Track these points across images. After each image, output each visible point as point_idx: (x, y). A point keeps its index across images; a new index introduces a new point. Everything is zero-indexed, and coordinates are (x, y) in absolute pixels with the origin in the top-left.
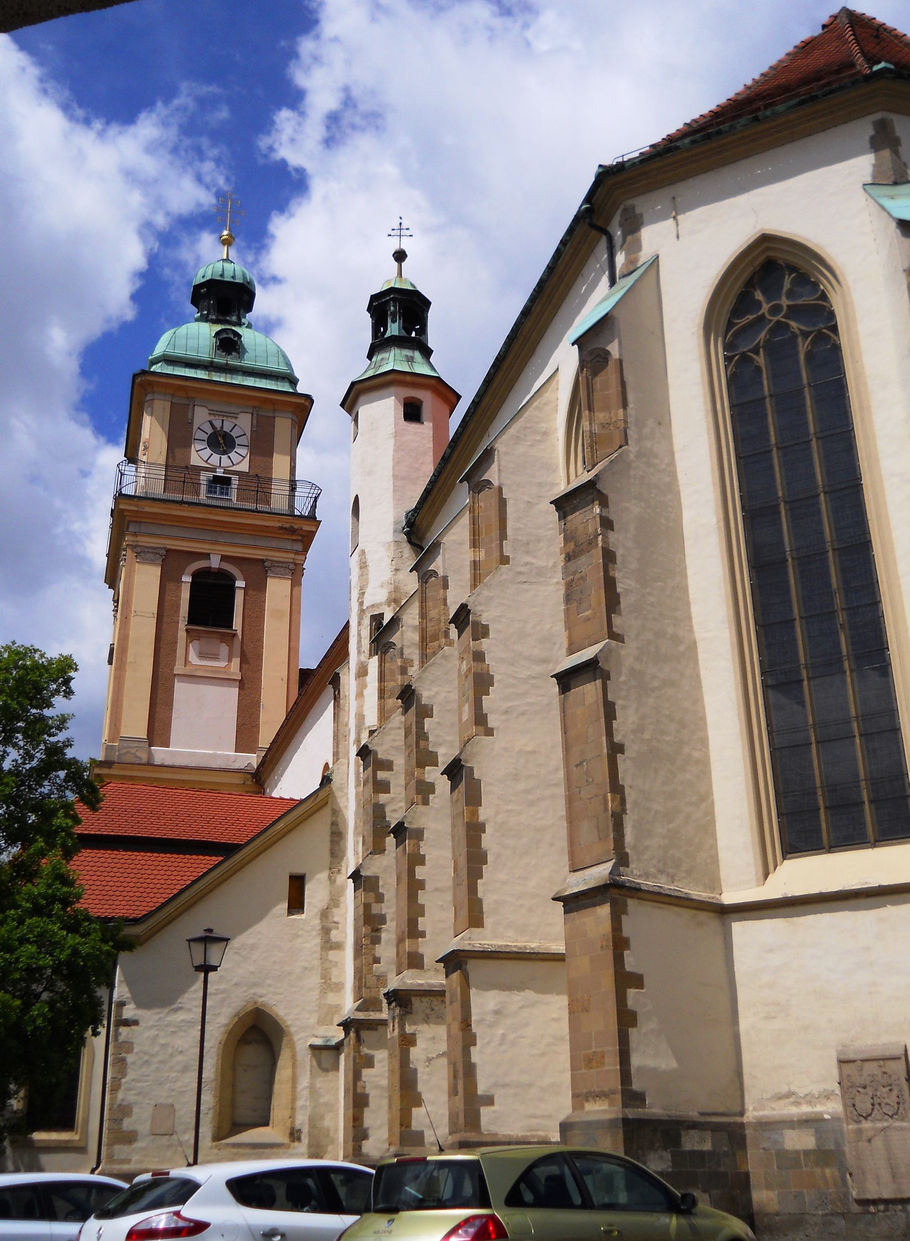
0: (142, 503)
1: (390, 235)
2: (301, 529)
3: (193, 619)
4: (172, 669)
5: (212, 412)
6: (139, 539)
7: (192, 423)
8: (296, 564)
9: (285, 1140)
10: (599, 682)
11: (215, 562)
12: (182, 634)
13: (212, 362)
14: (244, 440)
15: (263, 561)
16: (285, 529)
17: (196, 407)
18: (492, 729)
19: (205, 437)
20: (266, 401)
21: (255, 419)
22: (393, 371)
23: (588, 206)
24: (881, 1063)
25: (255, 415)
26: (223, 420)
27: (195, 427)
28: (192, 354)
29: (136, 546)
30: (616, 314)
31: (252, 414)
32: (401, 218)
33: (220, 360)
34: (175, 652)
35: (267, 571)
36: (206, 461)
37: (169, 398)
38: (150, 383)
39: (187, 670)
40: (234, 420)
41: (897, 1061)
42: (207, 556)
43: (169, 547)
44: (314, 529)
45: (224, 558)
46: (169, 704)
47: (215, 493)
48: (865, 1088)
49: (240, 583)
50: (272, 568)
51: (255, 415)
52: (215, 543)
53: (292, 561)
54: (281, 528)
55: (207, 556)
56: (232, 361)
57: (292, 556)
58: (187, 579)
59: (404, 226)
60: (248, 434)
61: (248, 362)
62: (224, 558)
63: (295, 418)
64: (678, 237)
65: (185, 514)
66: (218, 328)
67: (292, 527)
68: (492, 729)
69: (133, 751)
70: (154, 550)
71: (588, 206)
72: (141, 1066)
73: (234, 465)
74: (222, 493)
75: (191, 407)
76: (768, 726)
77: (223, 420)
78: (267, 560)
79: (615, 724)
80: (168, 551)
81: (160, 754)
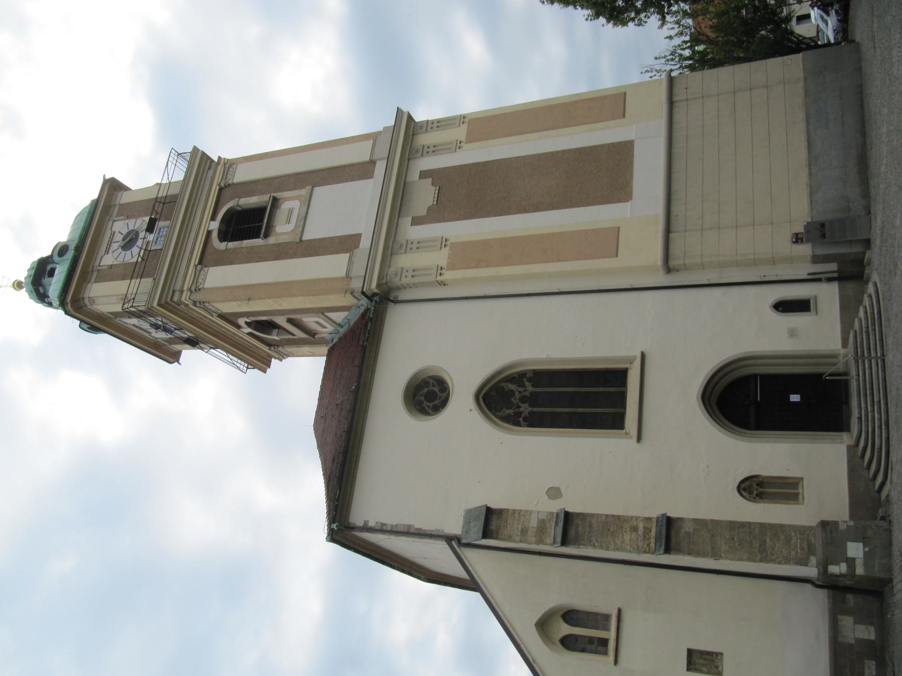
5: (107, 252)
6: (185, 288)
11: (215, 226)
15: (221, 189)
21: (118, 218)
27: (116, 263)
31: (114, 221)
35: (229, 185)
37: (89, 285)
40: (115, 235)
43: (197, 263)
44: (200, 154)
55: (209, 233)
57: (219, 167)
58: (223, 246)
62: (213, 218)
77: (114, 242)
78: (219, 185)
80: (200, 262)
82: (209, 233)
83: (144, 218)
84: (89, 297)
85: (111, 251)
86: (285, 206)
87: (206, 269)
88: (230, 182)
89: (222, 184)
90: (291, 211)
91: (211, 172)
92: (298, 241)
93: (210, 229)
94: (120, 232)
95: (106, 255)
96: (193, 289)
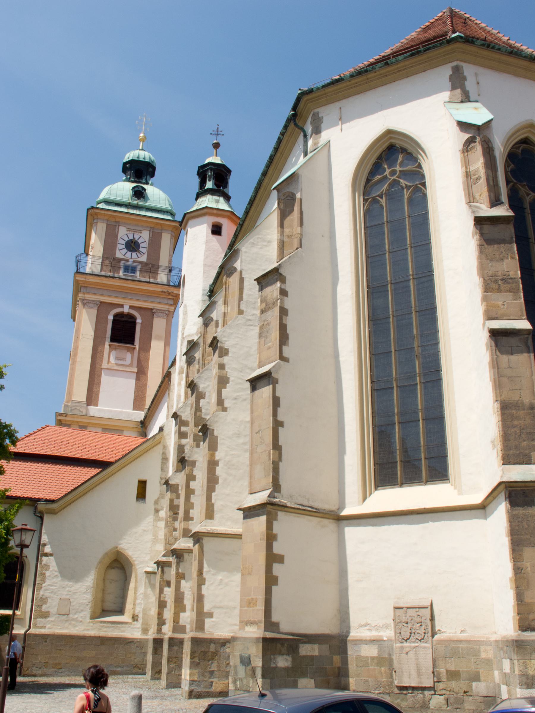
0: (88, 277)
1: (211, 134)
2: (173, 292)
3: (113, 339)
4: (101, 365)
5: (129, 230)
6: (86, 296)
7: (117, 235)
8: (169, 311)
9: (130, 620)
10: (271, 386)
11: (126, 310)
12: (107, 347)
13: (130, 203)
14: (145, 245)
15: (152, 309)
16: (165, 292)
17: (120, 227)
18: (226, 408)
19: (124, 242)
20: (157, 224)
21: (151, 233)
22: (206, 207)
23: (293, 112)
24: (417, 609)
25: (151, 232)
26: (134, 234)
27: (119, 238)
28: (119, 199)
29: (84, 300)
30: (300, 172)
31: (150, 231)
32: (218, 125)
33: (135, 202)
34: (103, 356)
36: (124, 255)
38: (96, 214)
39: (109, 366)
40: (140, 234)
41: (426, 609)
42: (122, 306)
45: (131, 307)
46: (99, 384)
47: (128, 272)
48: (407, 623)
49: (139, 321)
50: (157, 313)
51: (151, 232)
52: (127, 298)
53: (167, 309)
54: (162, 292)
56: (140, 203)
57: (167, 307)
58: (111, 317)
59: (220, 129)
60: (147, 241)
61: (149, 204)
62: (131, 307)
63: (173, 234)
64: (342, 130)
65: (111, 283)
66: (134, 185)
67: (168, 291)
68: (226, 408)
69: (78, 408)
70: (93, 302)
71: (293, 112)
72: (53, 578)
73: (138, 257)
74: (131, 273)
75: (117, 226)
76: (372, 412)
77: (134, 234)
79: (279, 409)
80: (101, 302)
81: (93, 410)
82: (122, 306)
83: (146, 255)
84: (97, 222)
85: (128, 232)
86: (129, 356)
87: (97, 307)
88: (155, 315)
89: (153, 311)
90: (124, 359)
91: (166, 301)
92: (102, 367)
93: (124, 306)
94: (141, 237)
95: (126, 229)
96: (85, 301)
